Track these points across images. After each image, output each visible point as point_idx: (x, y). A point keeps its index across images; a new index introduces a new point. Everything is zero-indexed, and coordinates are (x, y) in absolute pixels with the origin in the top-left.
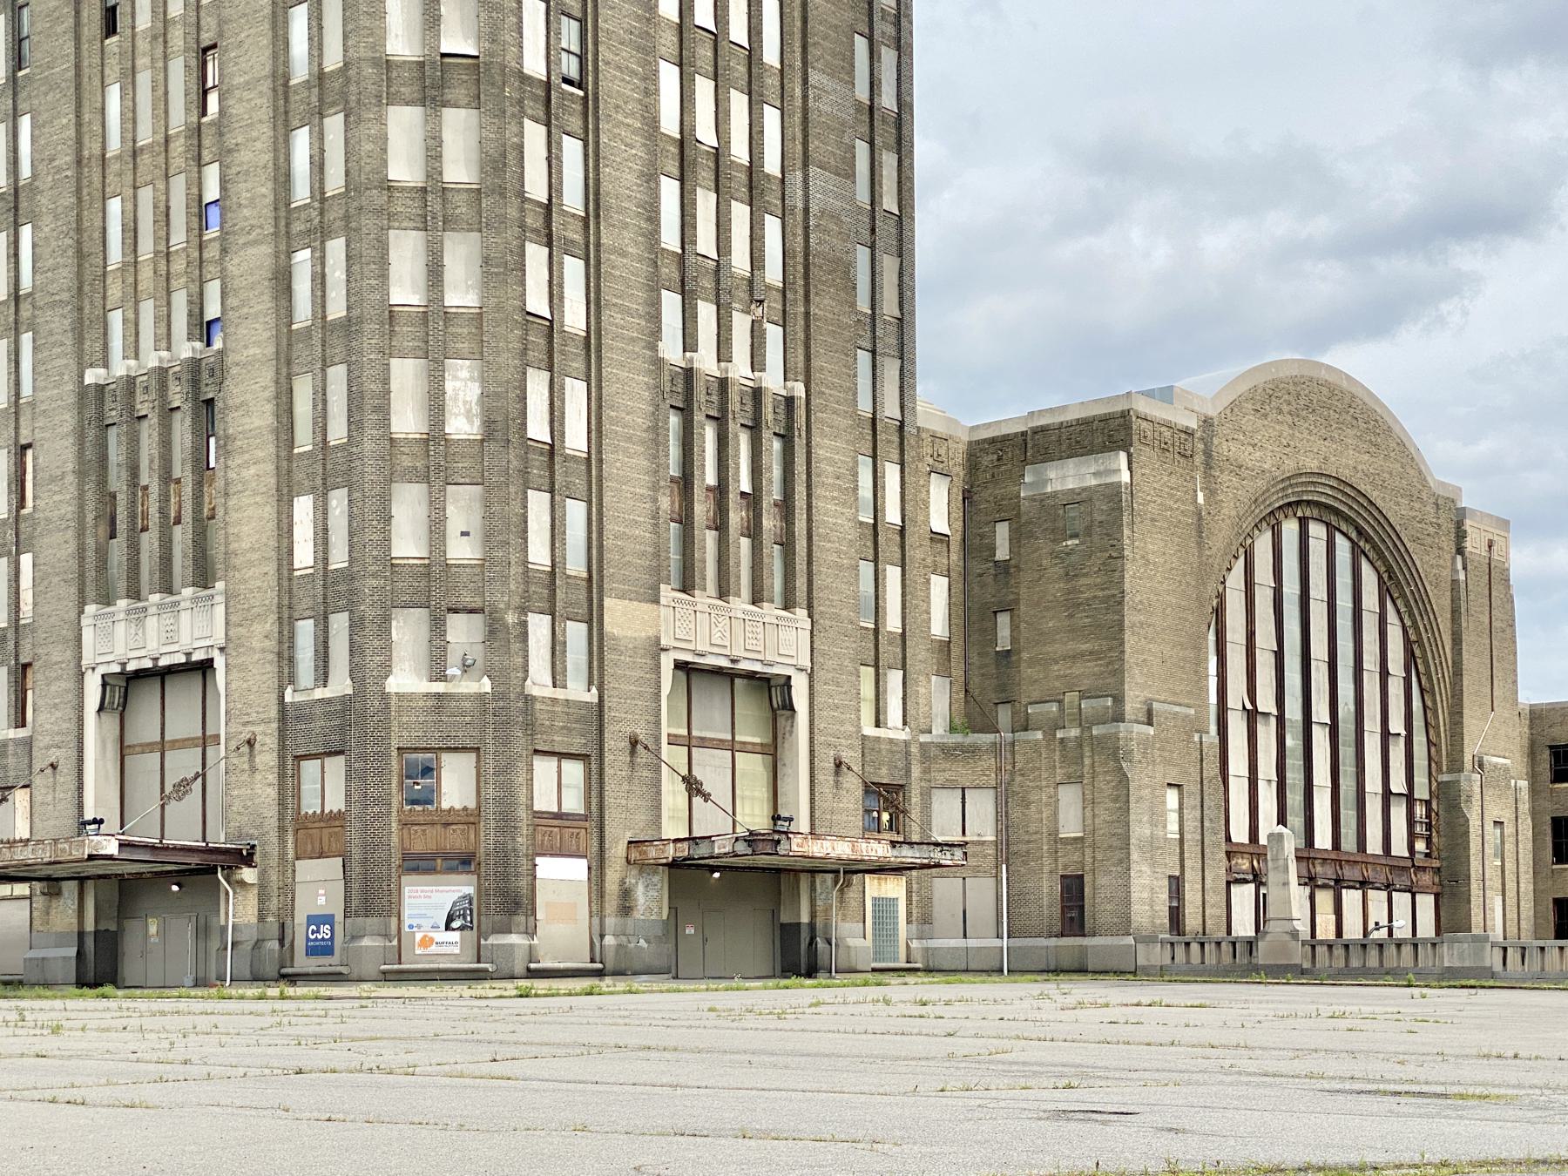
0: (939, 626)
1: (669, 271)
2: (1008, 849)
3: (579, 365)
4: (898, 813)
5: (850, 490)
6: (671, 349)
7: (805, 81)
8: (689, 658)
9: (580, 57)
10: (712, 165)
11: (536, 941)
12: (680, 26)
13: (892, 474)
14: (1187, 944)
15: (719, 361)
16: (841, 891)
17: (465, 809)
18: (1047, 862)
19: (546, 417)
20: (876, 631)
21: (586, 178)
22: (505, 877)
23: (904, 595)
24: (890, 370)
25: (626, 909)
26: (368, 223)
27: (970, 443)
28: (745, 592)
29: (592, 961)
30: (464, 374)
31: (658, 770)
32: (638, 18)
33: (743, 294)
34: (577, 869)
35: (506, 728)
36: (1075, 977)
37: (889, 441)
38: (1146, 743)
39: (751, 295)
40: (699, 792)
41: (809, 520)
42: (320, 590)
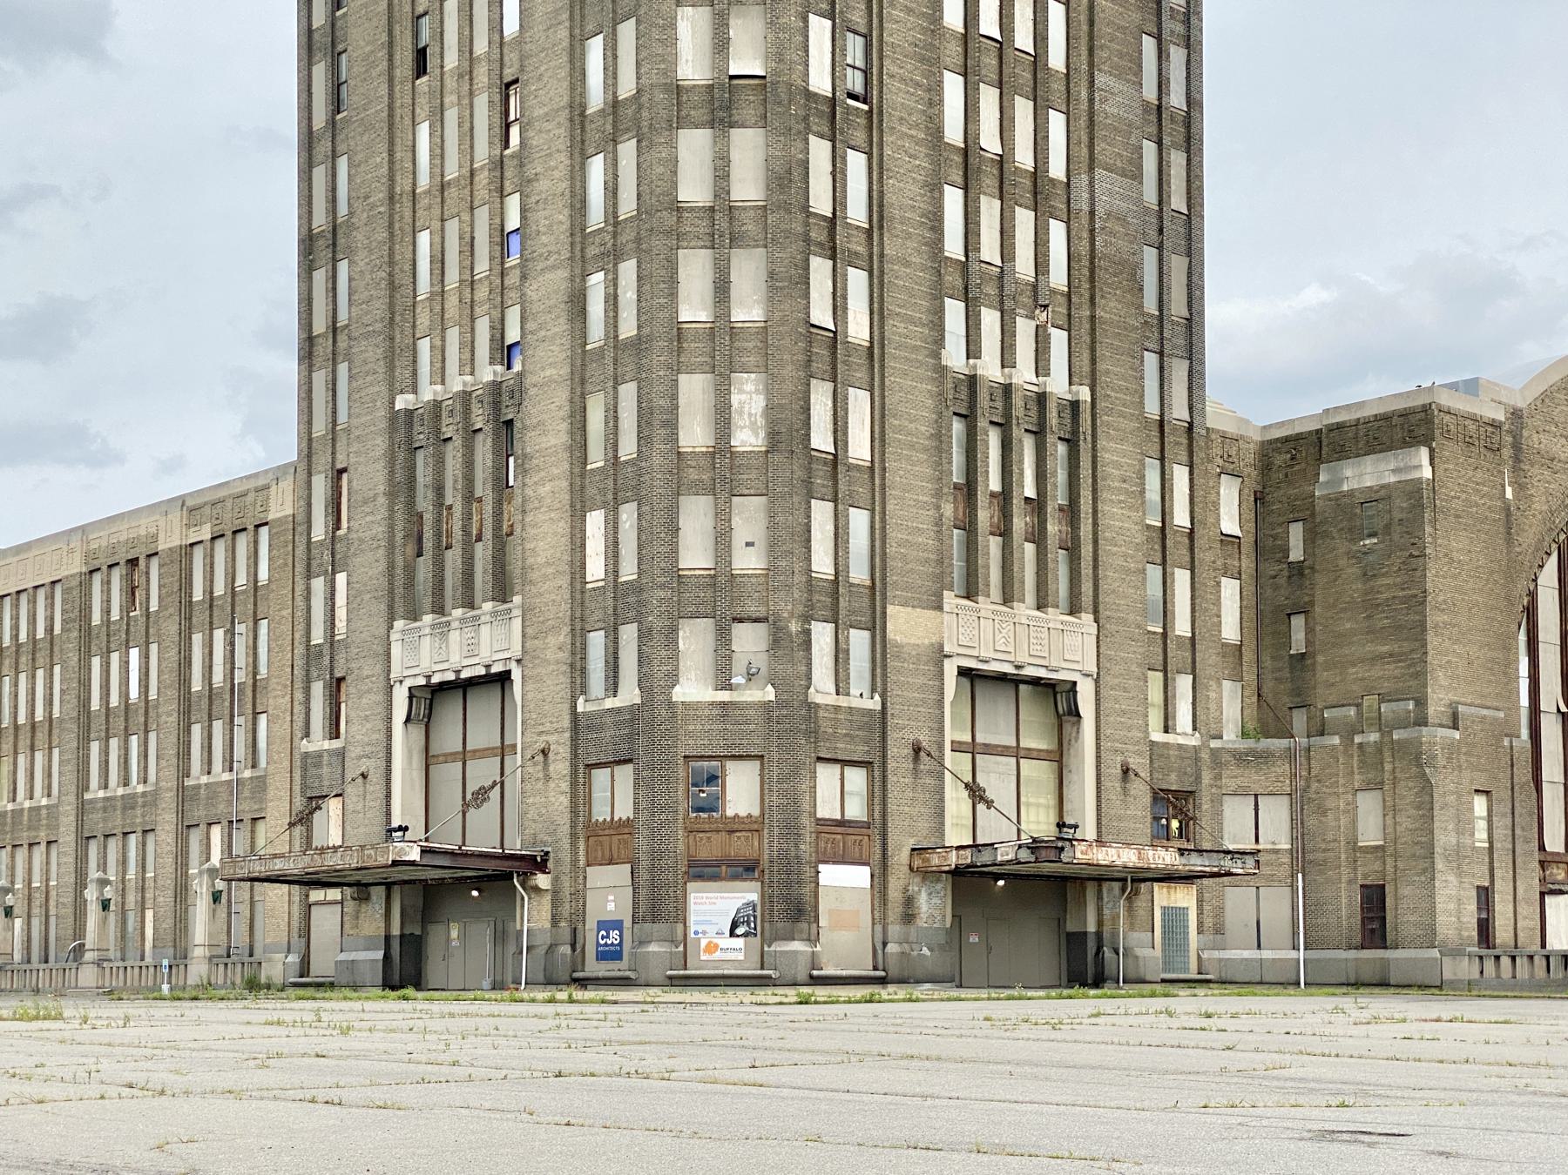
0: (1230, 630)
1: (953, 279)
2: (1304, 857)
3: (861, 374)
4: (1187, 821)
5: (1138, 492)
6: (954, 356)
7: (1092, 83)
8: (973, 664)
9: (865, 72)
10: (995, 172)
11: (819, 948)
12: (965, 36)
13: (1180, 475)
14: (1497, 958)
15: (1003, 367)
16: (1129, 898)
17: (750, 816)
18: (1345, 873)
19: (830, 427)
20: (1165, 635)
21: (870, 190)
22: (788, 885)
23: (1193, 598)
24: (1179, 370)
25: (909, 917)
26: (658, 243)
27: (1263, 443)
28: (1030, 597)
30: (750, 387)
31: (941, 778)
32: (924, 30)
33: (1026, 299)
35: (793, 735)
36: (1377, 990)
37: (1177, 443)
38: (1452, 748)
39: (1036, 300)
40: (982, 798)
41: (1095, 524)
42: (610, 602)
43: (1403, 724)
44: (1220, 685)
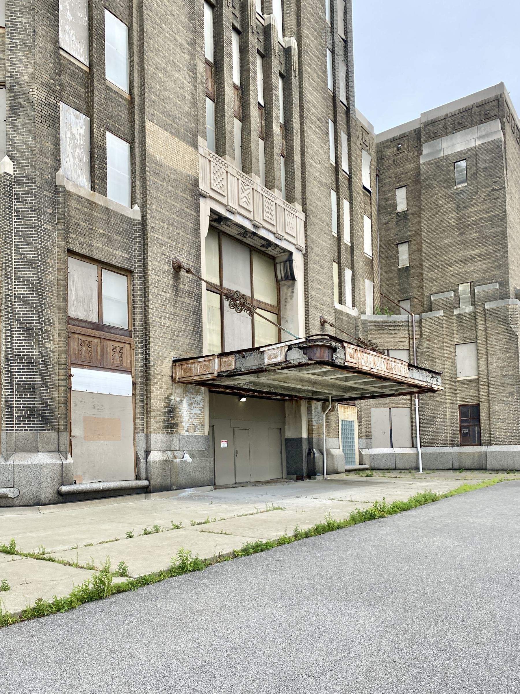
25: (171, 425)
29: (138, 477)
34: (121, 384)
43: (493, 298)
44: (364, 282)
